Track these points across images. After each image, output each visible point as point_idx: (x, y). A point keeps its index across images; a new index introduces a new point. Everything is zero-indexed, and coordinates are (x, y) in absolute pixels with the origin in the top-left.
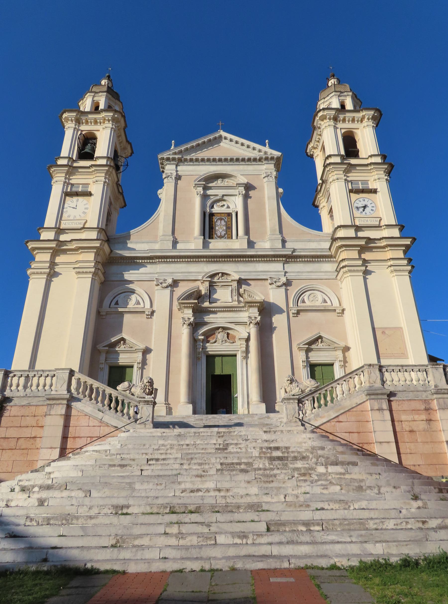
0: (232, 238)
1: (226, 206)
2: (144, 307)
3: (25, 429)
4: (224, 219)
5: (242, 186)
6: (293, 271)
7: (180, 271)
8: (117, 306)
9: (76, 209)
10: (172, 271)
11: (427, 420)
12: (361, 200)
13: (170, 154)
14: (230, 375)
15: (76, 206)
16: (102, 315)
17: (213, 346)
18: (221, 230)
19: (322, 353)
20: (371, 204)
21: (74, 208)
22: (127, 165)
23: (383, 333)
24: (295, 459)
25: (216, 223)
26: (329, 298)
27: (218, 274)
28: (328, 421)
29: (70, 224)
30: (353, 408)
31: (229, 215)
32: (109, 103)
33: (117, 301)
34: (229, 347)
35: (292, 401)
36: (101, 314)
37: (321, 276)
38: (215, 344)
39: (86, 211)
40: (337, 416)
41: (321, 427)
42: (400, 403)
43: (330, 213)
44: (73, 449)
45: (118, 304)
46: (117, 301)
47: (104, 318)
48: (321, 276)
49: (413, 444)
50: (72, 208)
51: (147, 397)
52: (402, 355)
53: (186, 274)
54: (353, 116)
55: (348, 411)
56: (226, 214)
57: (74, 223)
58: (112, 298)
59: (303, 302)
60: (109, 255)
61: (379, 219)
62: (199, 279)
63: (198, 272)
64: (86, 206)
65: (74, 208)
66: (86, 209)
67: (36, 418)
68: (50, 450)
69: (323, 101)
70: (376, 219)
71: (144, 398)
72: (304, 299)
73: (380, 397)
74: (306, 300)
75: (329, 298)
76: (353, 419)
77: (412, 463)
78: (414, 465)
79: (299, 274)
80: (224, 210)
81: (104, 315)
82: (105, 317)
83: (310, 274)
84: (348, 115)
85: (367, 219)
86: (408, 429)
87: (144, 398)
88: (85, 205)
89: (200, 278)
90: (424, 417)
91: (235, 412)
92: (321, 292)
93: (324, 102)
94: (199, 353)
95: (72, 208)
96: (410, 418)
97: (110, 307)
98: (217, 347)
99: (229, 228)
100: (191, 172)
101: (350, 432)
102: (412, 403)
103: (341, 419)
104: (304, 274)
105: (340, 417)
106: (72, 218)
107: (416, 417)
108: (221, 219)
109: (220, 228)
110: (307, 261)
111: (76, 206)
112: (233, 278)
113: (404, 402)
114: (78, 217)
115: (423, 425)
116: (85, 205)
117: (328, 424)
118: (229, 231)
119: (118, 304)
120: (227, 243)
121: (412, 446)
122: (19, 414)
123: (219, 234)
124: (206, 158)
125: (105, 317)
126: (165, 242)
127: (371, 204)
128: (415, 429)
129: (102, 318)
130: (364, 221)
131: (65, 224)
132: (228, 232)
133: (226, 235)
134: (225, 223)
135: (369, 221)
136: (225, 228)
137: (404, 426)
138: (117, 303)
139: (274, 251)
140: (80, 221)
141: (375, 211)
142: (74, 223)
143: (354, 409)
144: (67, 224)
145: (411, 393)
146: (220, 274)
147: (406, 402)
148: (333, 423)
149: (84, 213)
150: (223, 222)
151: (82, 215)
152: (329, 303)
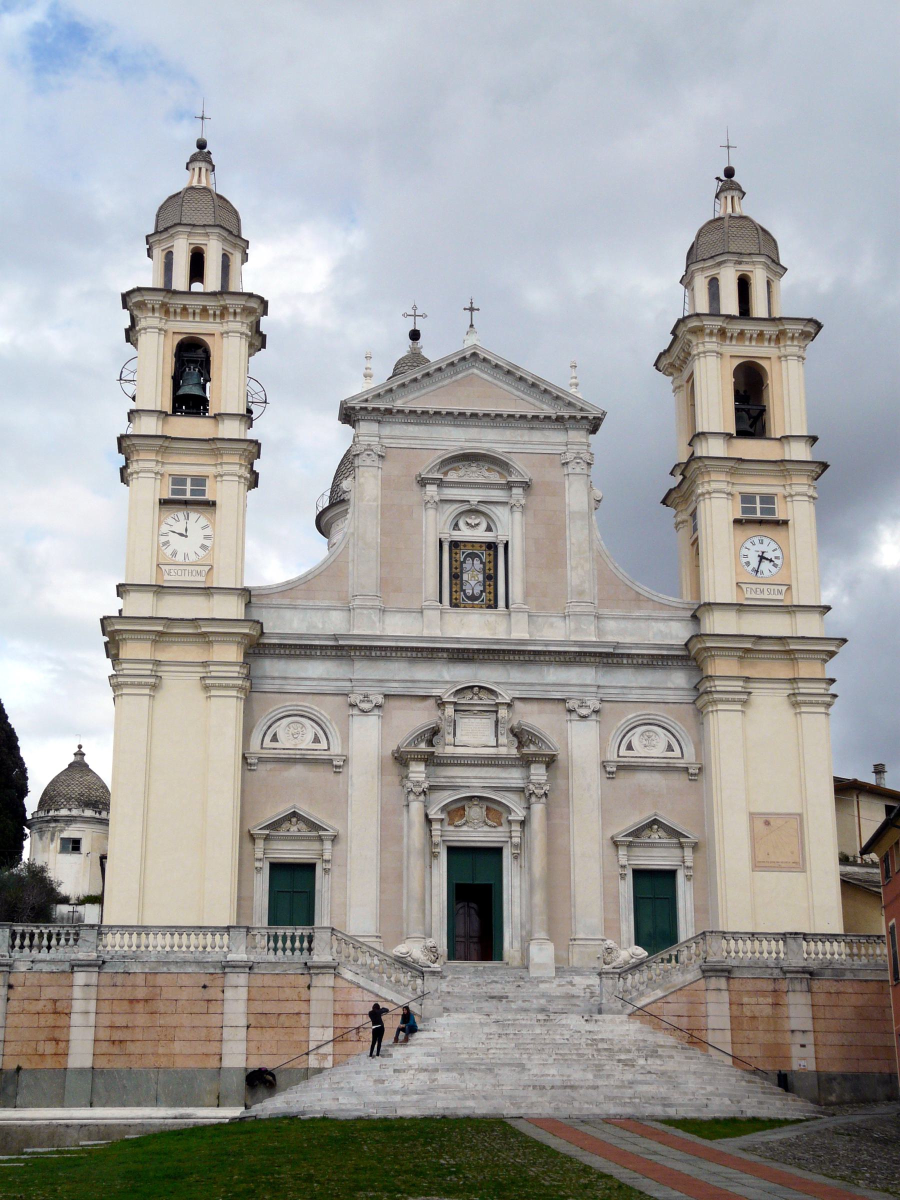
0: (496, 607)
1: (484, 525)
2: (329, 748)
3: (286, 1003)
4: (477, 556)
5: (520, 487)
6: (614, 684)
7: (397, 678)
8: (275, 745)
9: (186, 536)
10: (377, 677)
11: (773, 1004)
12: (756, 540)
13: (366, 401)
14: (491, 885)
15: (186, 530)
16: (251, 765)
17: (461, 831)
18: (473, 583)
19: (656, 852)
20: (774, 551)
21: (181, 535)
22: (265, 402)
23: (767, 823)
24: (620, 1051)
25: (464, 565)
26: (678, 741)
27: (472, 687)
28: (654, 1002)
29: (180, 572)
30: (685, 986)
31: (492, 546)
32: (223, 249)
33: (275, 735)
34: (490, 834)
35: (612, 976)
36: (249, 761)
37: (665, 697)
38: (465, 828)
39: (208, 543)
40: (665, 996)
41: (645, 1009)
42: (744, 981)
43: (693, 544)
44: (348, 1028)
45: (277, 741)
46: (275, 735)
47: (254, 770)
48: (665, 697)
49: (752, 1032)
50: (178, 534)
51: (432, 965)
52: (794, 865)
53: (409, 685)
54: (761, 331)
55: (680, 989)
56: (483, 545)
57: (187, 572)
58: (265, 728)
59: (630, 747)
60: (258, 639)
61: (785, 588)
62: (434, 694)
63: (431, 682)
64: (208, 532)
65: (181, 535)
66: (207, 537)
67: (297, 990)
68: (321, 1030)
69: (700, 265)
70: (780, 588)
71: (429, 967)
72: (630, 741)
73: (719, 974)
74: (635, 744)
75: (678, 741)
76: (684, 999)
77: (747, 1054)
78: (750, 1057)
79: (625, 691)
80: (480, 534)
81: (254, 764)
82: (255, 768)
83: (645, 691)
84: (750, 327)
85: (762, 587)
86: (749, 1014)
87: (429, 967)
88: (204, 528)
89: (436, 692)
90: (770, 1000)
91: (500, 958)
92: (664, 728)
93: (703, 268)
94: (437, 845)
95: (178, 534)
96: (753, 1000)
97: (262, 748)
98: (467, 834)
99: (491, 578)
100: (412, 442)
101: (678, 1016)
102: (758, 981)
103: (669, 999)
104: (634, 692)
105: (667, 997)
106: (180, 558)
107: (761, 1000)
108: (473, 556)
109: (473, 580)
110: (643, 664)
111: (186, 530)
112: (500, 700)
113: (748, 981)
114: (192, 558)
115: (768, 1010)
116: (204, 528)
117: (654, 1005)
118: (490, 585)
119: (277, 741)
120: (488, 616)
121: (751, 1034)
122: (274, 985)
123: (469, 592)
124: (444, 412)
125: (255, 768)
126: (365, 612)
127: (774, 551)
128: (757, 1014)
129: (250, 770)
130: (756, 592)
131: (169, 574)
132: (487, 587)
133: (484, 594)
134: (482, 566)
135: (765, 590)
136: (481, 577)
137: (744, 1010)
138: (275, 739)
139: (580, 646)
140: (199, 568)
141: (780, 568)
142: (187, 572)
143: (687, 988)
144: (173, 573)
145: (759, 969)
146: (476, 689)
147: (751, 980)
148: (659, 1004)
149: (204, 547)
150: (477, 562)
151: (202, 553)
152: (677, 753)
